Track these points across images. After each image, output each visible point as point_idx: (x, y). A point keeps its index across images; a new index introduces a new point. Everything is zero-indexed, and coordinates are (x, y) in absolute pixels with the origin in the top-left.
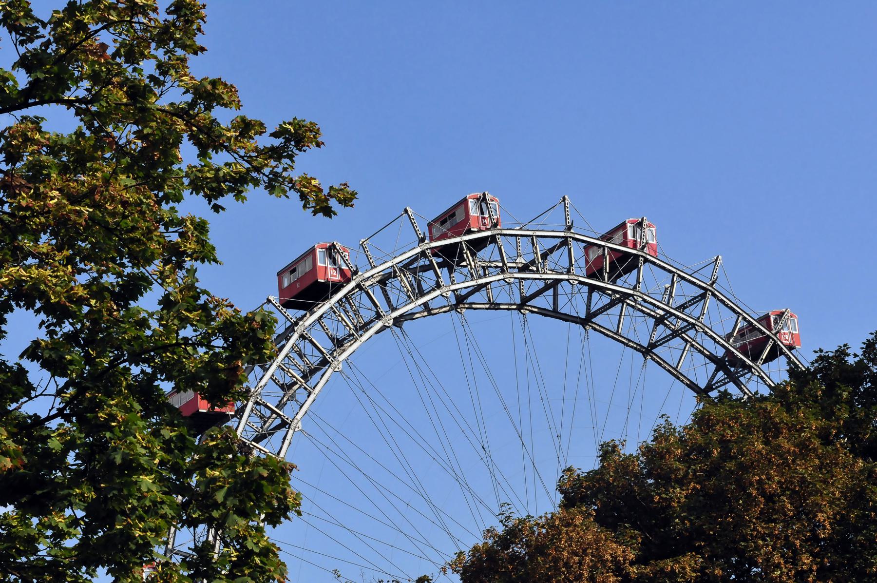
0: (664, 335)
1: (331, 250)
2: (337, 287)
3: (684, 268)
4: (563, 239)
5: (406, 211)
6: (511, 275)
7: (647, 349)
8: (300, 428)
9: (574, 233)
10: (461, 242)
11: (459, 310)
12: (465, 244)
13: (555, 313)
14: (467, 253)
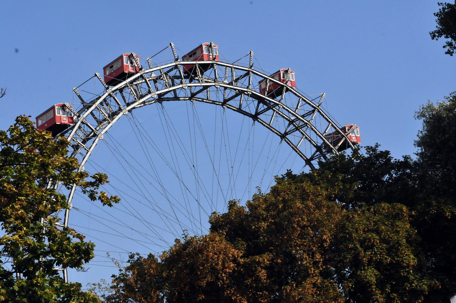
0: (293, 129)
1: (130, 57)
2: (131, 75)
3: (306, 96)
4: (247, 72)
5: (171, 45)
6: (219, 84)
7: (283, 135)
8: (102, 138)
9: (253, 70)
10: (196, 64)
11: (192, 100)
12: (198, 65)
14: (198, 71)
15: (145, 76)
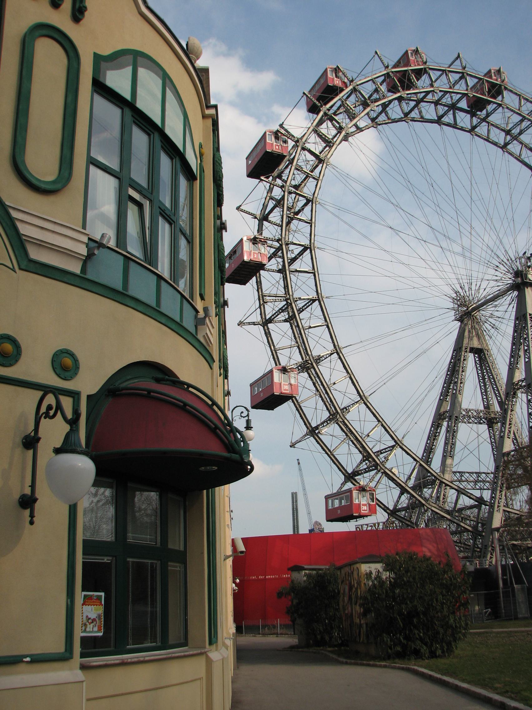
6: (437, 89)
13: (454, 126)
15: (359, 88)
